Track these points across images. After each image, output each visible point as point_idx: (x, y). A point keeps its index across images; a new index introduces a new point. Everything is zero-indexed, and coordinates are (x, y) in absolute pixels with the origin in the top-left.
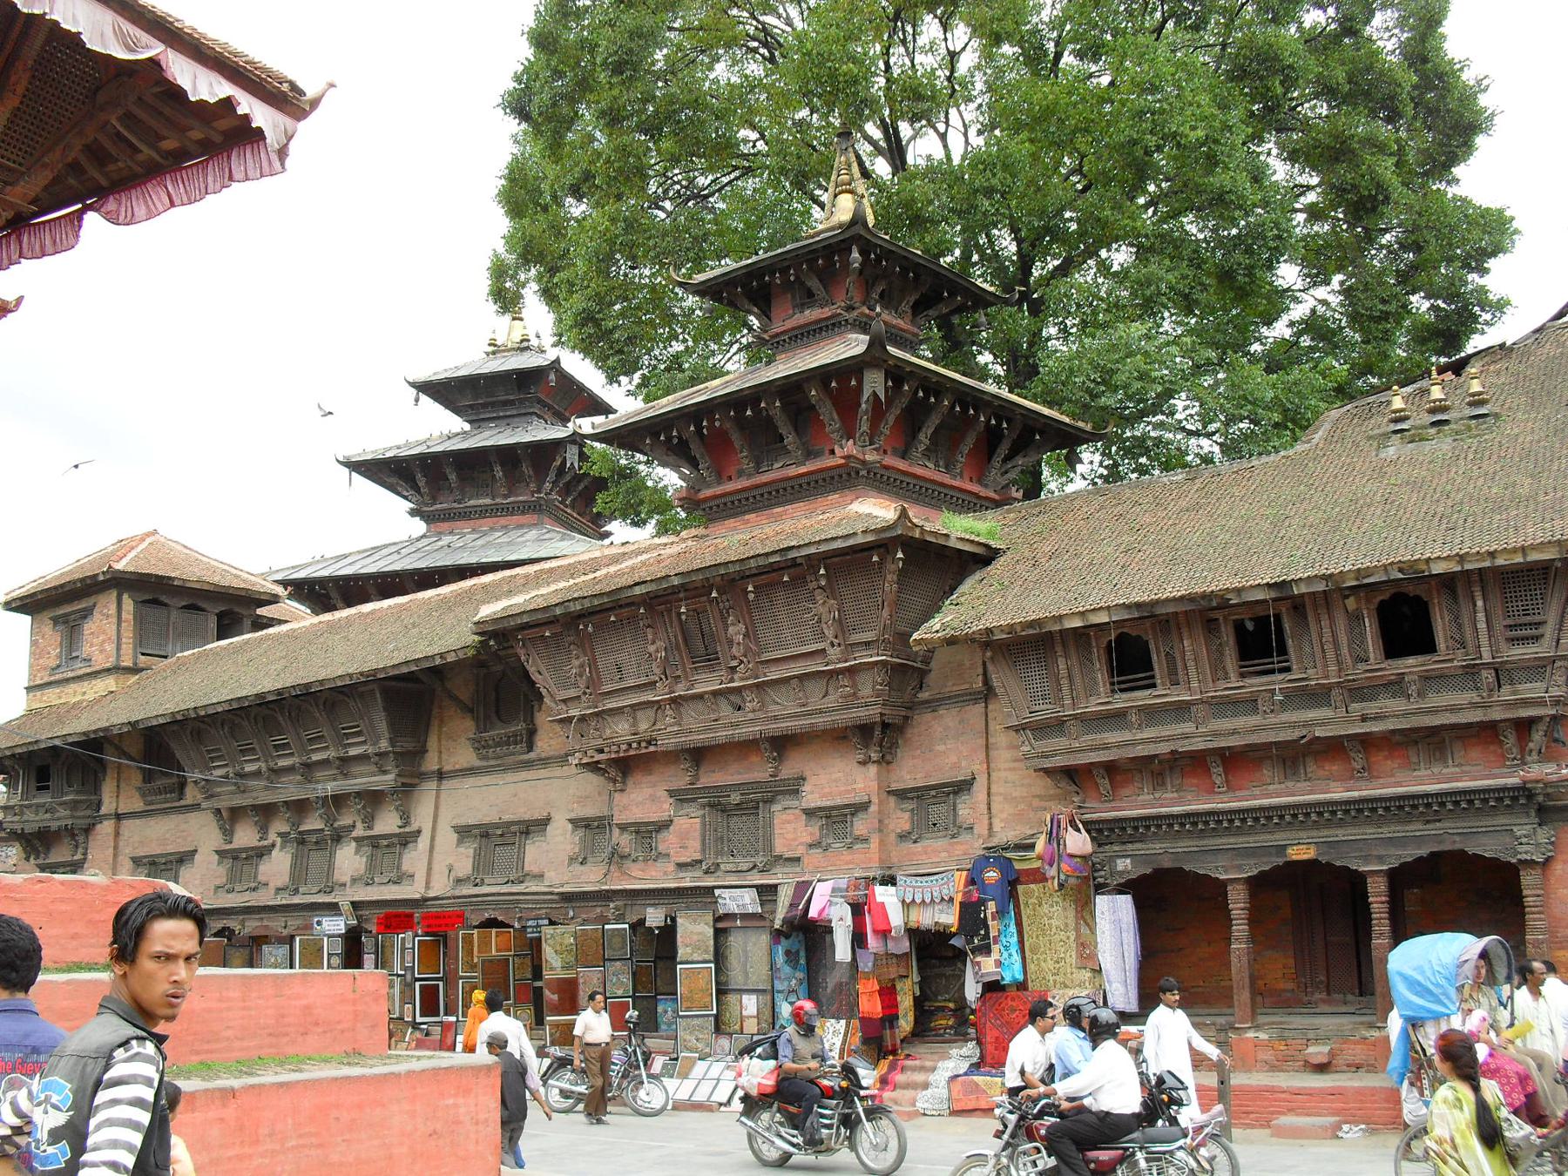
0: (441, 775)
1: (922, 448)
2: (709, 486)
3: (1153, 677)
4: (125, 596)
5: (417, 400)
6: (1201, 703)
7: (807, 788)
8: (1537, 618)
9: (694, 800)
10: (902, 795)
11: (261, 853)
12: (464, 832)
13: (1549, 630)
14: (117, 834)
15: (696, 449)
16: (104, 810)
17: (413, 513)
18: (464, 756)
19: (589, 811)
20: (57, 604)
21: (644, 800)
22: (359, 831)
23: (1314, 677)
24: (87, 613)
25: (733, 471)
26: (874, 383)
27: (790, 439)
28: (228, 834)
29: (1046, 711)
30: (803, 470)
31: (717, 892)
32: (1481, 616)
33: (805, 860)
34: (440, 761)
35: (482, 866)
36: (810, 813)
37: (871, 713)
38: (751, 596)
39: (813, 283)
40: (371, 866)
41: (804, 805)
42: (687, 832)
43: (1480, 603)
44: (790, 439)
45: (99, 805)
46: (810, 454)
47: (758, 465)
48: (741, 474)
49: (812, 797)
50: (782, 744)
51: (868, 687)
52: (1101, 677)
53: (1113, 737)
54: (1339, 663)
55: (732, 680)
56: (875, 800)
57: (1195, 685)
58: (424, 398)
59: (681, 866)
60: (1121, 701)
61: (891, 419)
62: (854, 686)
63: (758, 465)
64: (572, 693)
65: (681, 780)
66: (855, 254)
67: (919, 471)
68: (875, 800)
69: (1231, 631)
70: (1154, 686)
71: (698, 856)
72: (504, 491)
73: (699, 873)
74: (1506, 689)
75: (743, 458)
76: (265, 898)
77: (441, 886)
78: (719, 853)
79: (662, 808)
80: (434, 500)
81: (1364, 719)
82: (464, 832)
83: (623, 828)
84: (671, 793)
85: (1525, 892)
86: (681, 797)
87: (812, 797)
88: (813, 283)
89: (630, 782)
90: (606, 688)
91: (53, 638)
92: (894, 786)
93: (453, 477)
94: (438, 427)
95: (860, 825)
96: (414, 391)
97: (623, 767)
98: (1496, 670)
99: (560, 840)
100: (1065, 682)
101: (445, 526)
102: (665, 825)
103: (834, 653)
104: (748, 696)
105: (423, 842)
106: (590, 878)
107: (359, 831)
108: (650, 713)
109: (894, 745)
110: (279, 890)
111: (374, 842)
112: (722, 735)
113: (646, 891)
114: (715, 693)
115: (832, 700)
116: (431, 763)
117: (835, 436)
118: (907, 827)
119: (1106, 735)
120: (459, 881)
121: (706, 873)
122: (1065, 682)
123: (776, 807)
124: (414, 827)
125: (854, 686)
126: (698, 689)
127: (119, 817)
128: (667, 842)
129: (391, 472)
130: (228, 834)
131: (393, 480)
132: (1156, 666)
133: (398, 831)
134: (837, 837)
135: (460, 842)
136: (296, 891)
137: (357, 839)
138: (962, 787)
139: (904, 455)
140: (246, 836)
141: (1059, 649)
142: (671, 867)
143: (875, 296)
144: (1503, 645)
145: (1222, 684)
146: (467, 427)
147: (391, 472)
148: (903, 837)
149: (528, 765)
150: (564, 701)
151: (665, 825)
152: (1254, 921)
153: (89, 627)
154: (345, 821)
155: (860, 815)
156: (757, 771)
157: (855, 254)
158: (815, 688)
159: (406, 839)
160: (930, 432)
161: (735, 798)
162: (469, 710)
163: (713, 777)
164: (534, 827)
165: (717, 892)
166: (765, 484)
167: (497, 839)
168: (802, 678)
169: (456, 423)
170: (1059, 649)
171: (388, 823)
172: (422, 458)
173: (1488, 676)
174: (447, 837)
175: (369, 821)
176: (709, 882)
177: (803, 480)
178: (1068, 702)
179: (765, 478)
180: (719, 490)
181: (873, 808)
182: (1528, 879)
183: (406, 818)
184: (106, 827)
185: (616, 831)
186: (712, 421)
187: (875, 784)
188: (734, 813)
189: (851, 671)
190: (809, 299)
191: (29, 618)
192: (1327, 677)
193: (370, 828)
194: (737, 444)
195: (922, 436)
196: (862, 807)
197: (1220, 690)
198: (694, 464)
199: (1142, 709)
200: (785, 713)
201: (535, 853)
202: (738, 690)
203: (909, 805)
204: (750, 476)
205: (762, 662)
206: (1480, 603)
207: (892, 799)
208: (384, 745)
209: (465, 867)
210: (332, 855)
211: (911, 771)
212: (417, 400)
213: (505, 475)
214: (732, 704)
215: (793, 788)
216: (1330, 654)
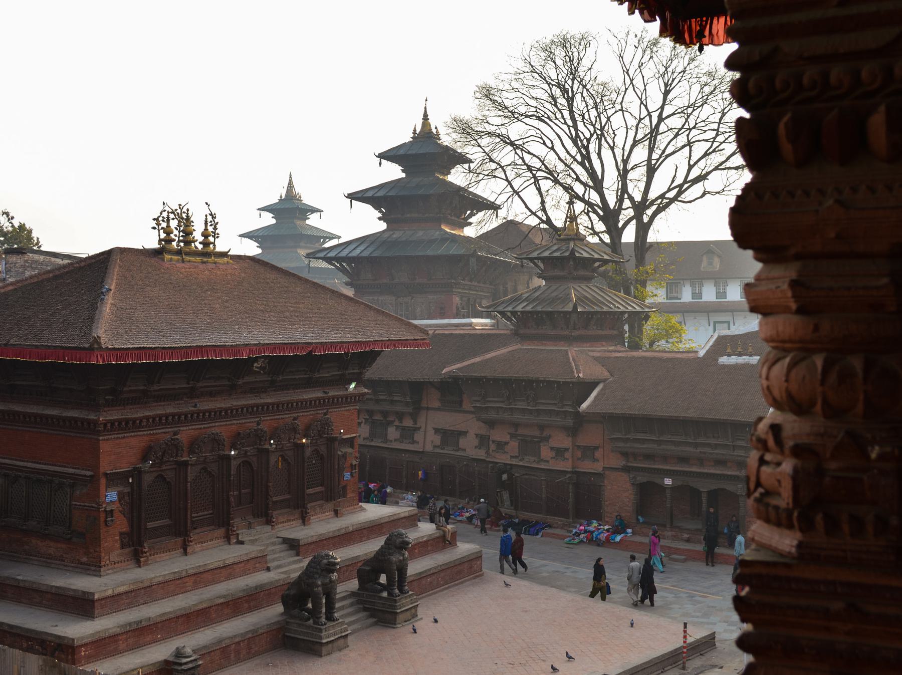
0: (428, 409)
5: (380, 164)
12: (437, 431)
17: (380, 219)
18: (437, 404)
21: (499, 435)
22: (397, 423)
36: (552, 448)
40: (402, 436)
49: (554, 443)
58: (383, 161)
59: (512, 457)
77: (429, 448)
79: (507, 438)
82: (437, 431)
83: (493, 442)
86: (513, 436)
87: (554, 443)
95: (567, 455)
102: (507, 443)
105: (423, 429)
106: (481, 454)
110: (364, 439)
111: (404, 429)
116: (424, 405)
120: (435, 447)
124: (418, 426)
135: (435, 433)
138: (596, 448)
148: (579, 459)
149: (460, 412)
151: (507, 443)
154: (390, 419)
167: (449, 436)
171: (408, 423)
174: (431, 432)
175: (401, 420)
181: (570, 450)
183: (415, 422)
196: (567, 450)
201: (462, 442)
208: (408, 399)
209: (438, 442)
210: (386, 429)
211: (582, 441)
212: (380, 164)
215: (547, 439)
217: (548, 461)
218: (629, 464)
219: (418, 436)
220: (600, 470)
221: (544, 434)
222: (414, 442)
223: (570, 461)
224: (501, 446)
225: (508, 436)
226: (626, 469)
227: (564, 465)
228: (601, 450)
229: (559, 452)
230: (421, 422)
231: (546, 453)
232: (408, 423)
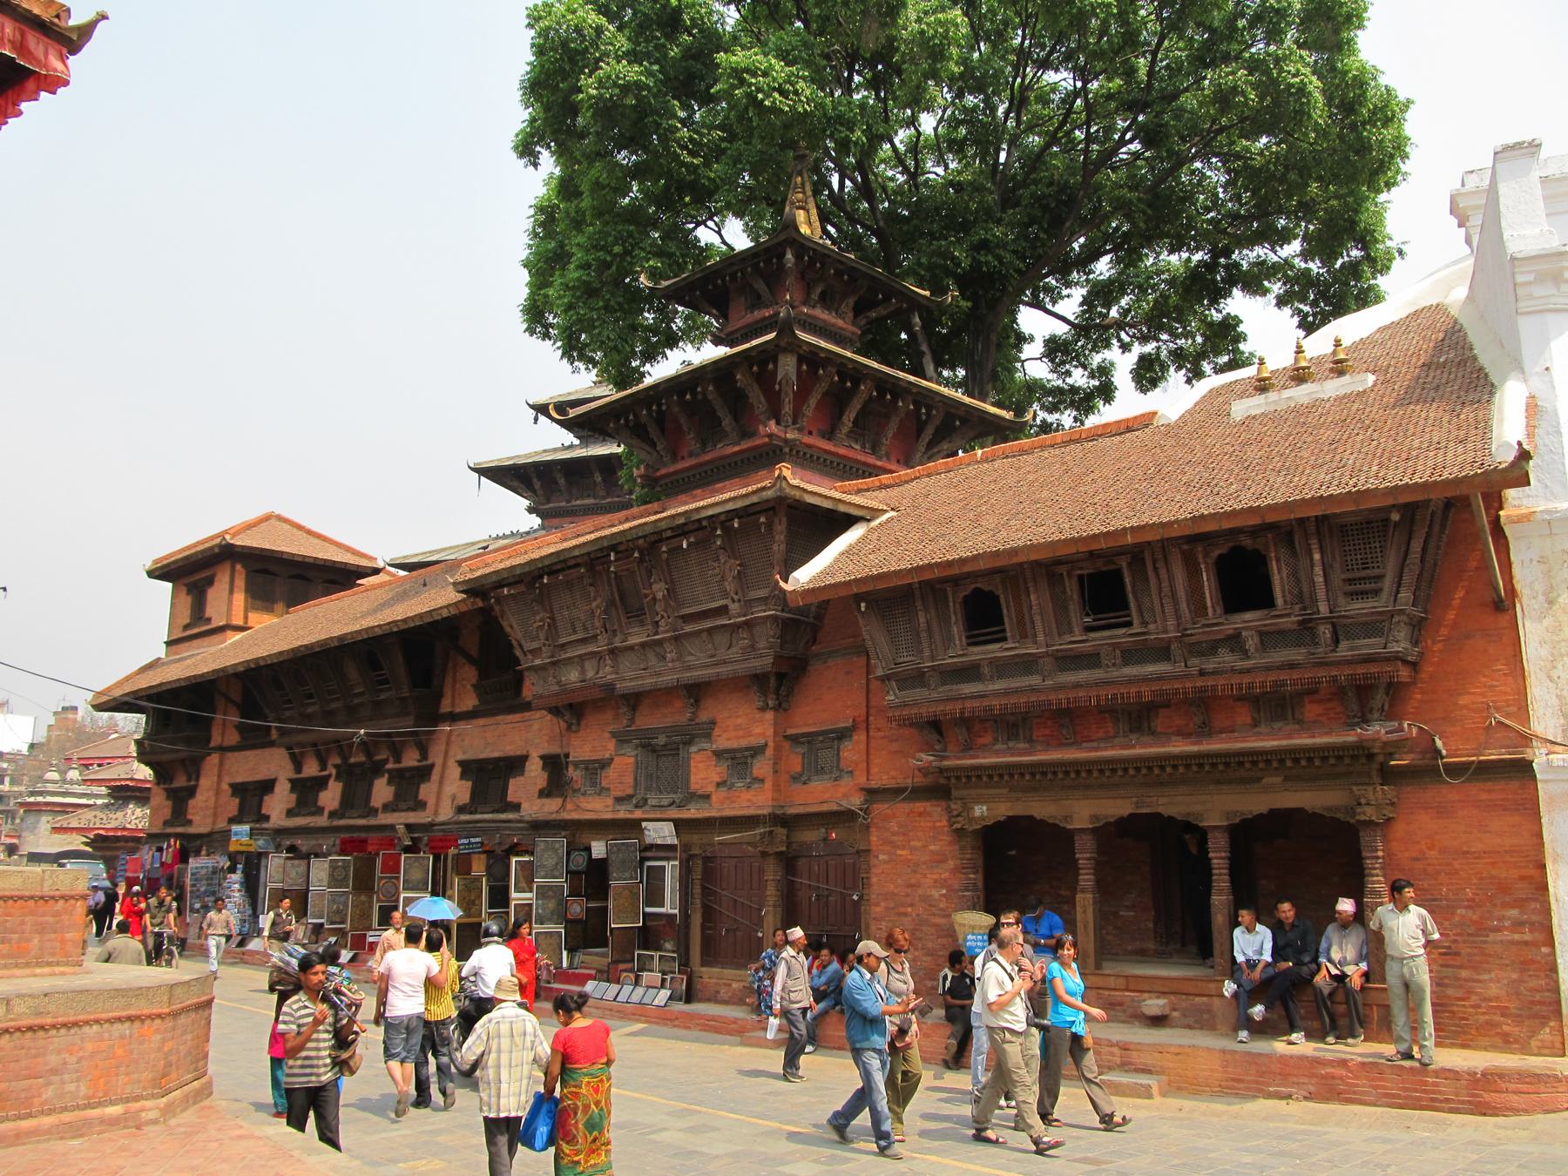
0: (454, 718)
1: (845, 430)
2: (665, 466)
3: (1004, 631)
4: (238, 567)
5: (536, 420)
6: (1045, 654)
7: (716, 733)
8: (1376, 572)
9: (629, 741)
10: (795, 739)
11: (322, 783)
13: (1388, 584)
14: (221, 764)
15: (654, 432)
16: (212, 745)
17: (530, 510)
18: (469, 702)
19: (554, 749)
20: (190, 573)
22: (390, 766)
23: (1154, 632)
24: (210, 582)
26: (787, 367)
27: (727, 422)
28: (298, 767)
29: (907, 659)
30: (737, 449)
31: (644, 824)
32: (1318, 570)
33: (714, 798)
34: (453, 705)
35: (479, 800)
36: (718, 754)
37: (764, 662)
39: (760, 286)
42: (624, 768)
43: (1317, 556)
44: (727, 422)
45: (209, 742)
46: (746, 434)
47: (704, 444)
48: (691, 455)
49: (725, 739)
50: (696, 692)
51: (766, 640)
52: (957, 630)
53: (968, 688)
54: (1178, 617)
55: (656, 633)
56: (771, 744)
57: (1041, 638)
58: (542, 418)
59: (619, 800)
60: (978, 653)
61: (813, 402)
62: (752, 637)
63: (704, 444)
64: (535, 645)
66: (789, 256)
67: (842, 451)
68: (771, 744)
69: (1075, 587)
70: (1004, 639)
71: (630, 791)
72: (602, 493)
73: (630, 807)
74: (1343, 645)
75: (690, 441)
76: (322, 821)
78: (648, 789)
80: (549, 501)
81: (1202, 673)
83: (576, 764)
84: (614, 735)
85: (1365, 854)
86: (622, 738)
88: (760, 286)
89: (583, 723)
90: (563, 640)
91: (186, 601)
92: (791, 731)
93: (562, 481)
94: (553, 440)
95: (762, 767)
96: (532, 413)
98: (1334, 625)
99: (535, 772)
100: (924, 635)
101: (556, 521)
102: (604, 764)
103: (734, 608)
104: (667, 645)
105: (435, 775)
106: (549, 808)
107: (390, 766)
108: (594, 662)
109: (789, 693)
112: (649, 682)
114: (643, 645)
115: (734, 653)
117: (762, 417)
118: (798, 769)
119: (962, 686)
120: (461, 810)
121: (637, 806)
122: (924, 635)
123: (693, 749)
124: (429, 762)
125: (752, 637)
126: (634, 640)
127: (222, 749)
128: (610, 776)
129: (511, 476)
130: (298, 767)
131: (515, 484)
132: (1006, 620)
133: (416, 764)
134: (742, 777)
136: (342, 816)
137: (390, 771)
138: (842, 735)
139: (829, 434)
140: (311, 769)
141: (919, 604)
142: (610, 801)
143: (815, 296)
144: (1341, 600)
145: (1068, 638)
146: (577, 442)
147: (511, 476)
148: (796, 778)
151: (604, 764)
152: (1099, 867)
153: (212, 593)
155: (759, 757)
157: (789, 256)
158: (722, 639)
159: (424, 773)
160: (852, 416)
161: (662, 740)
162: (471, 660)
164: (515, 765)
165: (644, 824)
166: (708, 462)
168: (710, 631)
169: (568, 438)
170: (919, 604)
172: (536, 465)
173: (1325, 632)
176: (638, 814)
177: (738, 458)
178: (927, 654)
179: (707, 457)
180: (672, 469)
181: (769, 752)
182: (1365, 837)
184: (214, 759)
186: (659, 406)
187: (770, 732)
188: (664, 756)
189: (748, 625)
190: (757, 302)
191: (170, 585)
192: (1166, 632)
193: (398, 761)
194: (685, 428)
195: (845, 418)
196: (757, 751)
197: (1062, 645)
198: (653, 445)
199: (992, 662)
200: (698, 663)
202: (660, 643)
203: (800, 750)
204: (697, 456)
205: (683, 617)
206: (1317, 556)
207: (787, 745)
209: (464, 797)
210: (371, 785)
212: (536, 420)
213: (604, 480)
214: (657, 655)
215: (707, 732)
216: (1169, 609)
217: (707, 797)
218: (946, 763)
219: (427, 791)
220: (855, 802)
221: (703, 717)
222: (421, 805)
223: (768, 784)
225: (611, 745)
226: (938, 788)
227: (753, 801)
228: (860, 737)
229: (739, 761)
230: (436, 756)
231: (703, 771)
232: (411, 759)
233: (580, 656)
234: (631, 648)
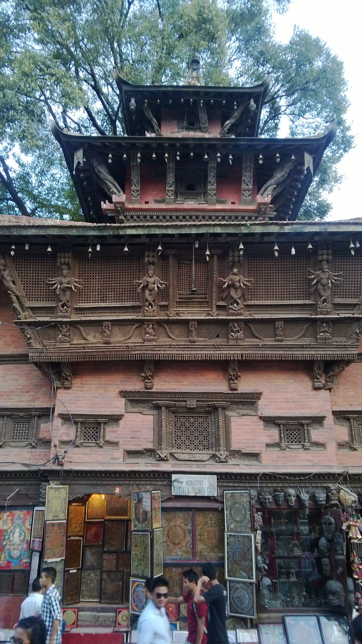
25: (150, 198)
31: (174, 477)
36: (269, 421)
38: (276, 254)
41: (259, 413)
42: (138, 427)
49: (267, 407)
59: (131, 453)
65: (135, 385)
79: (118, 406)
83: (66, 418)
84: (123, 394)
87: (267, 407)
88: (203, 117)
95: (316, 434)
97: (58, 372)
102: (115, 419)
113: (100, 472)
150: (32, 309)
151: (115, 419)
156: (214, 384)
163: (164, 384)
165: (174, 477)
176: (165, 467)
185: (58, 422)
215: (250, 400)
217: (255, 456)
224: (92, 427)
229: (294, 429)
233: (112, 321)
234: (186, 322)
